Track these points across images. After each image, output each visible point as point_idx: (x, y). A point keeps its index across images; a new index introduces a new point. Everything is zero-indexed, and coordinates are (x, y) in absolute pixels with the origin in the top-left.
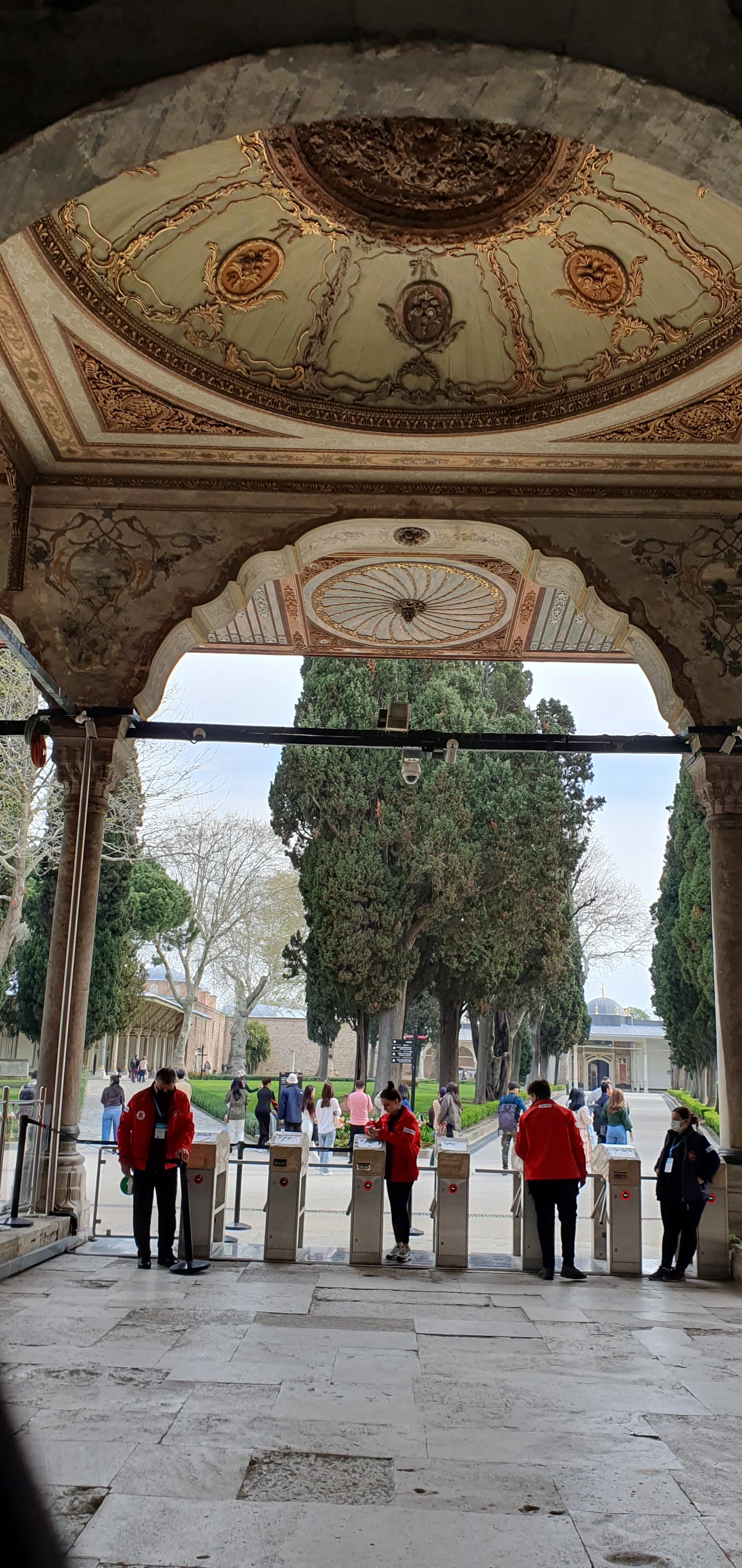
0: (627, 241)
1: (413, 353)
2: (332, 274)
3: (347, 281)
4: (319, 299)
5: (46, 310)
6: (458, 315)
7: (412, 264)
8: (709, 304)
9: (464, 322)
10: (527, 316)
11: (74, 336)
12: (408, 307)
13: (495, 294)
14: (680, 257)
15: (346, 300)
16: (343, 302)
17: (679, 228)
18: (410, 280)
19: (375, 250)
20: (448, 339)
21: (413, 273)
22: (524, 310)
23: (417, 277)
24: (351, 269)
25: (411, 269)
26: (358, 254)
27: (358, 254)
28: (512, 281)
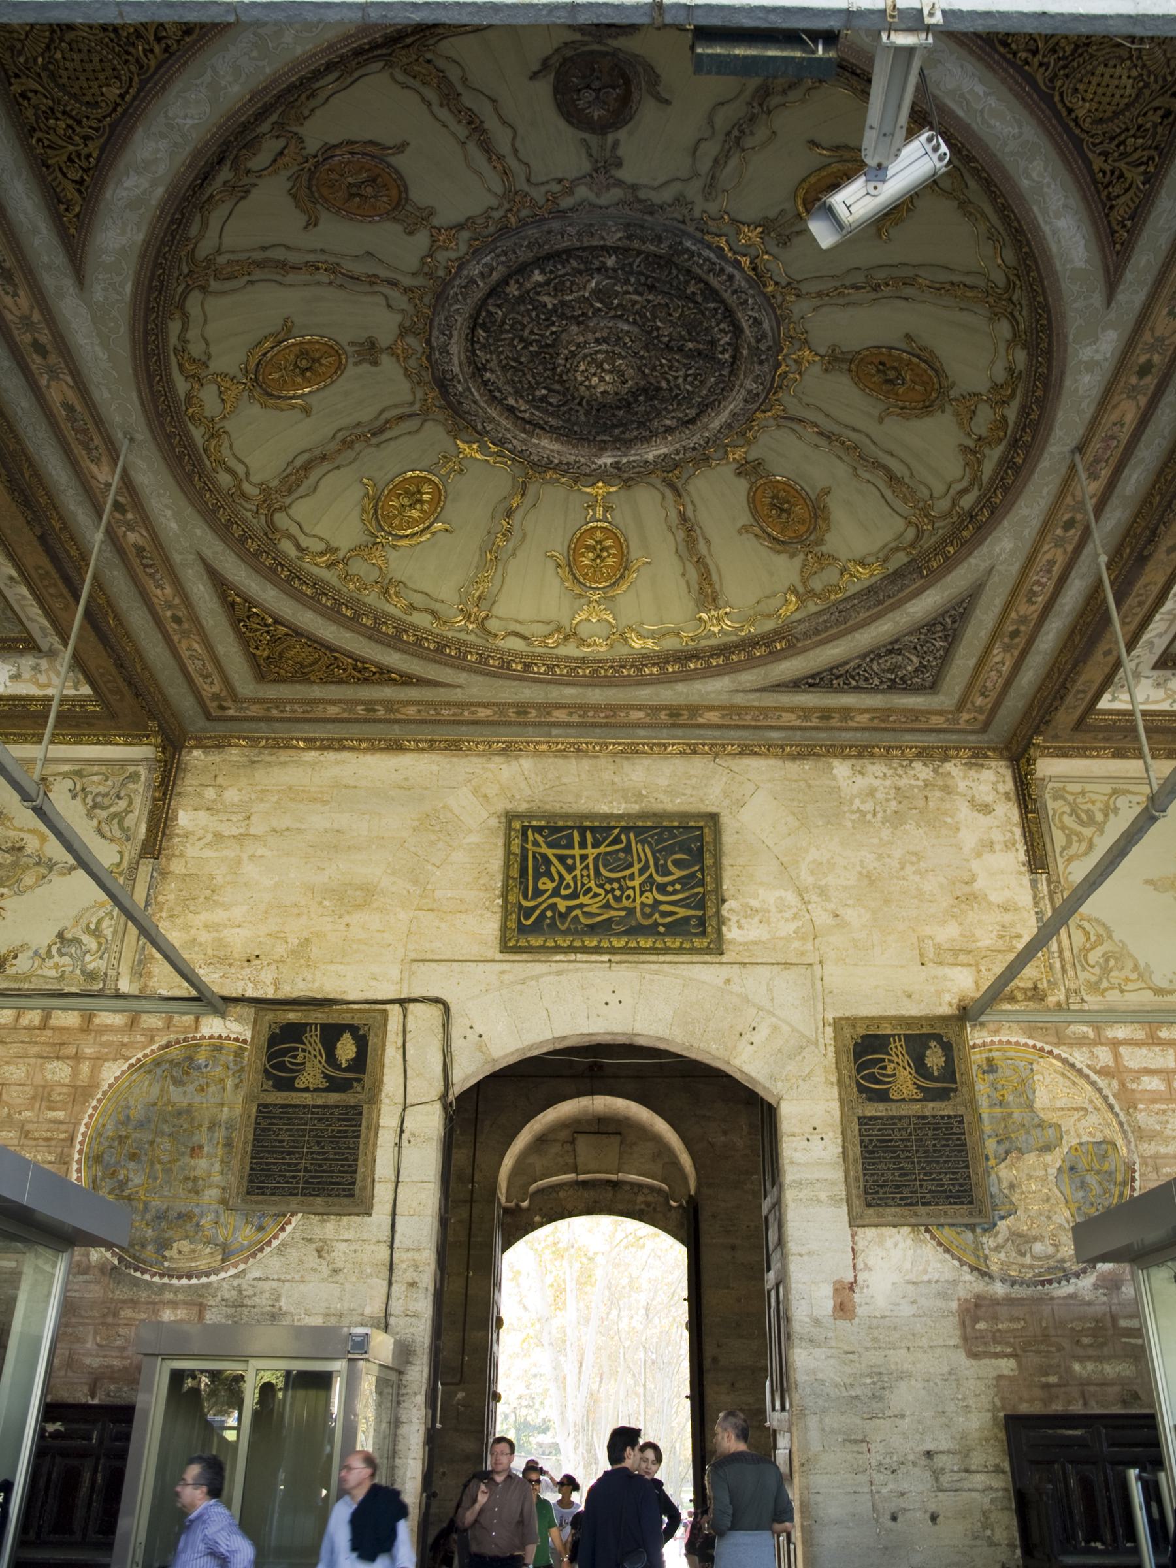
0: (339, 235)
1: (615, 43)
2: (733, 162)
3: (711, 149)
4: (761, 133)
5: (1112, 315)
6: (544, 88)
7: (619, 165)
8: (205, 249)
9: (531, 78)
10: (435, 108)
11: (1107, 271)
12: (626, 100)
13: (492, 124)
14: (269, 254)
15: (719, 120)
16: (722, 120)
17: (291, 278)
18: (622, 134)
19: (667, 195)
20: (555, 61)
21: (616, 144)
22: (444, 114)
23: (610, 138)
24: (705, 166)
25: (620, 152)
26: (693, 191)
27: (693, 191)
28: (472, 147)
